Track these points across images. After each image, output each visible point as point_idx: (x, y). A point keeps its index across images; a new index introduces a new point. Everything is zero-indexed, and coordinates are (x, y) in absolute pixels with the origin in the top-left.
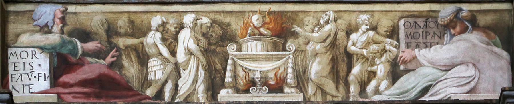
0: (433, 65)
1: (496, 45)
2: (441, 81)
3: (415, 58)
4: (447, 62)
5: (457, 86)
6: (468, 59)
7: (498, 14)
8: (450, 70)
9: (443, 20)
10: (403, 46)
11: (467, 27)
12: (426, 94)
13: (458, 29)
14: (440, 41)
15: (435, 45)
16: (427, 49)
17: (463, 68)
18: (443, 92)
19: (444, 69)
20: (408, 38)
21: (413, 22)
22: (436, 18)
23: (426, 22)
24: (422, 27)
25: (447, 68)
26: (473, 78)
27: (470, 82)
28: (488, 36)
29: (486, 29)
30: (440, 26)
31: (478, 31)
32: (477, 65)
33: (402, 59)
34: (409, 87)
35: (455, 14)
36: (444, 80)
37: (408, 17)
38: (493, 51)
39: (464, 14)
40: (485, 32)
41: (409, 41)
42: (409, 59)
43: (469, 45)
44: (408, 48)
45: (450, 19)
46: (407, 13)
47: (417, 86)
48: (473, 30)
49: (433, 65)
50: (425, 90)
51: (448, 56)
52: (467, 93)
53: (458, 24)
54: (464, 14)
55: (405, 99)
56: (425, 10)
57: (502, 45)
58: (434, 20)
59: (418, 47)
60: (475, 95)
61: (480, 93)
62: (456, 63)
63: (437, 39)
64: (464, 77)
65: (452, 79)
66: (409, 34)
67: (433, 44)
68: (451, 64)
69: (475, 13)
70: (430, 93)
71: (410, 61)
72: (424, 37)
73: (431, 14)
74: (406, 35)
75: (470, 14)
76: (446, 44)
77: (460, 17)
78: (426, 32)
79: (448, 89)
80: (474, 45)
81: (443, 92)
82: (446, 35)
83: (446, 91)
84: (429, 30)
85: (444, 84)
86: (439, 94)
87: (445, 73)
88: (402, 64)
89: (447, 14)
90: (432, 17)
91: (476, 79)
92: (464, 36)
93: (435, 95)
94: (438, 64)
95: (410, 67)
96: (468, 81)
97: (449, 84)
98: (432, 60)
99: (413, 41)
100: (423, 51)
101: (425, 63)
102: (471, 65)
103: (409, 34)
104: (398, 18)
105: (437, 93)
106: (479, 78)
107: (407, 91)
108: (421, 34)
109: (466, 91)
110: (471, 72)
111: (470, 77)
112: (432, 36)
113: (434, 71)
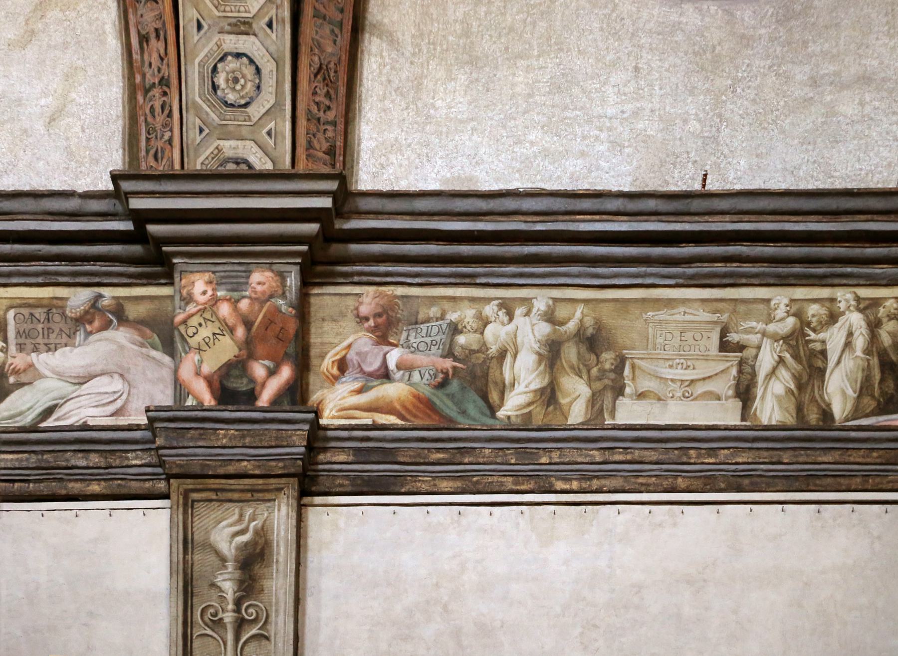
0: (60, 376)
1: (154, 347)
2: (72, 398)
3: (31, 365)
4: (81, 372)
5: (96, 406)
6: (112, 368)
7: (157, 302)
8: (86, 382)
9: (73, 311)
10: (13, 348)
11: (111, 321)
12: (48, 418)
13: (97, 324)
14: (70, 342)
15: (62, 347)
16: (50, 353)
17: (105, 379)
18: (75, 414)
19: (77, 381)
20: (21, 337)
21: (28, 314)
22: (63, 308)
23: (48, 314)
24: (42, 321)
25: (81, 381)
26: (119, 394)
27: (115, 400)
28: (143, 335)
29: (139, 324)
30: (69, 321)
31: (127, 327)
32: (126, 375)
33: (12, 367)
34: (24, 408)
35: (92, 302)
36: (77, 397)
37: (20, 306)
38: (149, 356)
39: (105, 302)
40: (136, 329)
41: (22, 342)
42: (22, 368)
43: (114, 347)
44: (21, 352)
45: (84, 309)
46: (18, 301)
47: (35, 407)
48: (119, 325)
49: (60, 376)
50: (48, 412)
51: (83, 363)
52: (112, 415)
53: (97, 317)
54: (105, 302)
55: (16, 425)
56: (47, 296)
57: (163, 346)
58: (60, 311)
59: (36, 350)
60: (122, 418)
61: (130, 416)
62: (94, 373)
63: (65, 339)
64: (106, 393)
65: (88, 396)
66: (21, 332)
67: (58, 346)
68: (86, 374)
69: (121, 301)
70: (54, 416)
71: (25, 370)
72: (46, 336)
73: (55, 302)
74: (18, 332)
75: (113, 302)
76: (79, 345)
77: (100, 306)
78: (48, 329)
79: (82, 410)
80: (122, 347)
81: (75, 414)
82: (78, 333)
83: (80, 413)
84: (51, 325)
85: (75, 403)
86: (68, 418)
87: (77, 387)
88: (11, 374)
89: (80, 302)
90: (57, 307)
91: (124, 397)
92: (105, 334)
93: (63, 420)
94: (67, 375)
95: (24, 378)
96: (112, 399)
97: (83, 403)
98: (57, 369)
99: (28, 341)
100: (44, 356)
101: (47, 373)
102: (116, 376)
103: (21, 332)
104: (4, 308)
105: (67, 415)
106: (129, 394)
107: (20, 414)
108: (41, 331)
109: (109, 414)
110: (117, 385)
111: (115, 392)
112: (58, 334)
113: (62, 384)
